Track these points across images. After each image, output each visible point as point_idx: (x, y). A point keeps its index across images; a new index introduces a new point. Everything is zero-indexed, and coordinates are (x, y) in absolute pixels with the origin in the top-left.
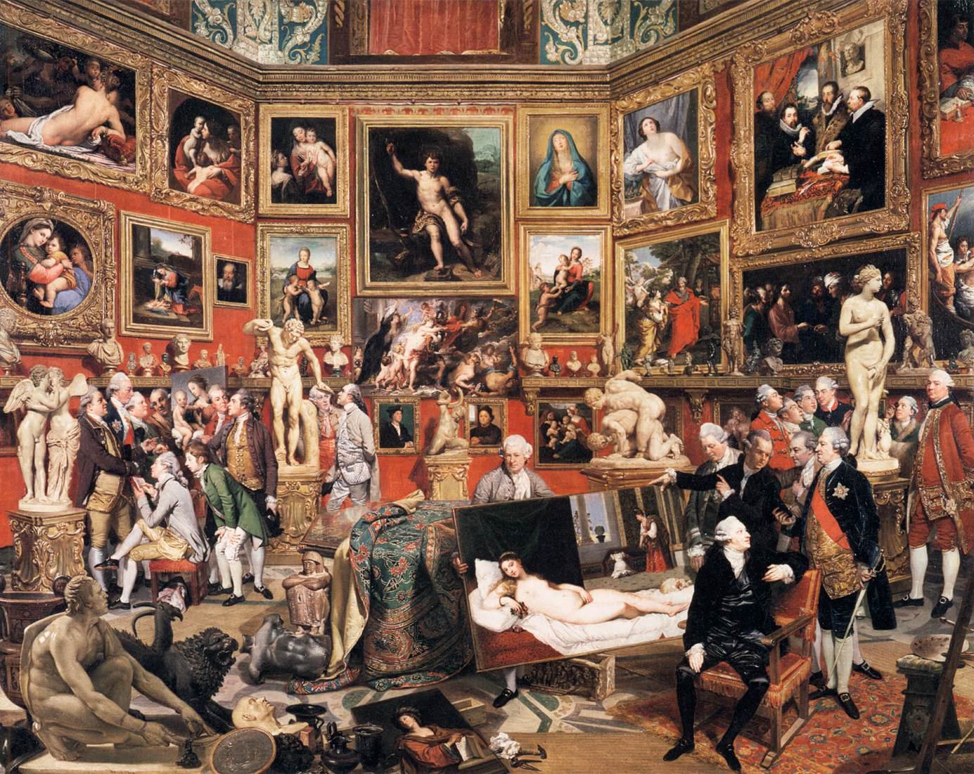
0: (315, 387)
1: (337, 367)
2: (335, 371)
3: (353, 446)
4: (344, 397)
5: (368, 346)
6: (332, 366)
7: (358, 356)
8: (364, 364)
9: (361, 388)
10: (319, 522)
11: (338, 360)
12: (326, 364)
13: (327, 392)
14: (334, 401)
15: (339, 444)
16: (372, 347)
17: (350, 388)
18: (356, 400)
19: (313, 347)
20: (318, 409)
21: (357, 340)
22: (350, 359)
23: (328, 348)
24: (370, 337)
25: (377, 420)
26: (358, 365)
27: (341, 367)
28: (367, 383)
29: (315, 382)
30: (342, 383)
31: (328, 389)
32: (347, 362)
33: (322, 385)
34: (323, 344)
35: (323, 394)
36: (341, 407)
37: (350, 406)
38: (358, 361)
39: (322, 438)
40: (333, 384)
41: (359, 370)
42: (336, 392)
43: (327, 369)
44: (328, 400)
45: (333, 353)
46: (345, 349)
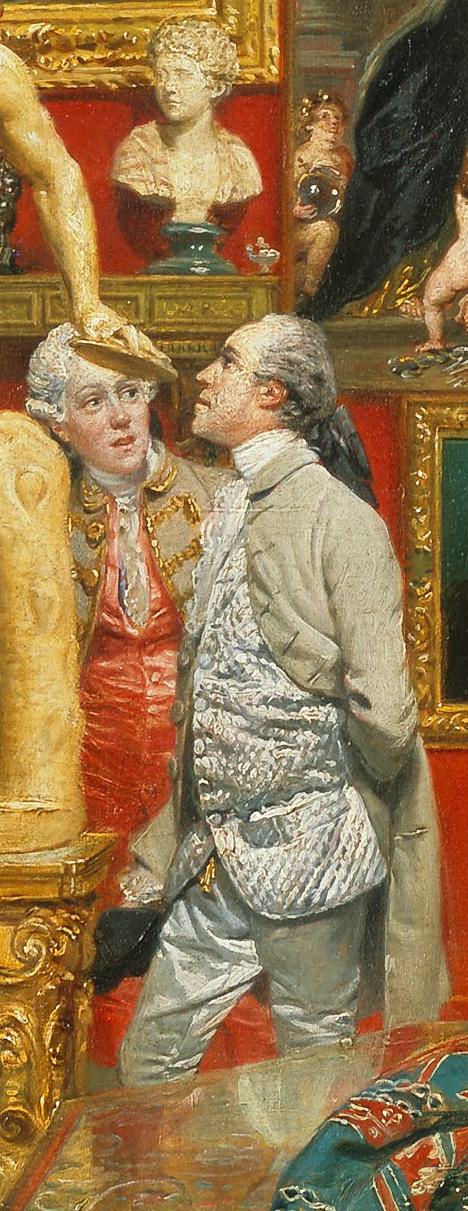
0: (63, 332)
1: (191, 215)
2: (184, 240)
3: (282, 687)
4: (230, 392)
5: (379, 95)
6: (166, 207)
7: (319, 149)
8: (354, 198)
9: (337, 342)
10: (78, 1149)
11: (196, 172)
12: (127, 195)
13: (130, 365)
14: (171, 417)
15: (201, 678)
16: (402, 104)
17: (267, 338)
18: (299, 409)
19: (55, 99)
20: (77, 468)
21: (309, 57)
22: (273, 164)
23: (141, 104)
24: (393, 35)
25: (425, 536)
26: (321, 202)
27: (221, 214)
28: (364, 314)
29: (64, 307)
30: (223, 308)
31: (138, 342)
32: (252, 183)
33: (100, 320)
34: (112, 77)
35: (107, 376)
36: (215, 453)
37: (269, 448)
38: (320, 178)
39: (100, 640)
40: (169, 313)
41: (321, 233)
42: (190, 366)
43: (135, 230)
44: (137, 410)
45: (171, 131)
46: (255, 113)
